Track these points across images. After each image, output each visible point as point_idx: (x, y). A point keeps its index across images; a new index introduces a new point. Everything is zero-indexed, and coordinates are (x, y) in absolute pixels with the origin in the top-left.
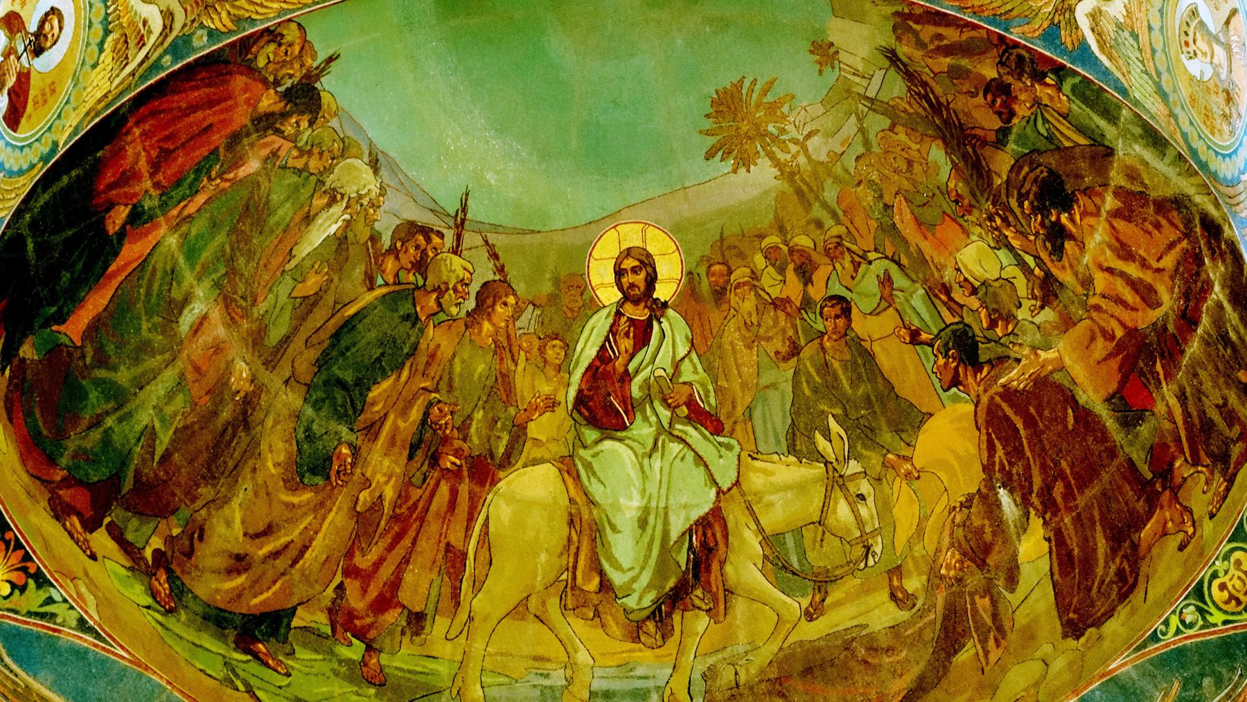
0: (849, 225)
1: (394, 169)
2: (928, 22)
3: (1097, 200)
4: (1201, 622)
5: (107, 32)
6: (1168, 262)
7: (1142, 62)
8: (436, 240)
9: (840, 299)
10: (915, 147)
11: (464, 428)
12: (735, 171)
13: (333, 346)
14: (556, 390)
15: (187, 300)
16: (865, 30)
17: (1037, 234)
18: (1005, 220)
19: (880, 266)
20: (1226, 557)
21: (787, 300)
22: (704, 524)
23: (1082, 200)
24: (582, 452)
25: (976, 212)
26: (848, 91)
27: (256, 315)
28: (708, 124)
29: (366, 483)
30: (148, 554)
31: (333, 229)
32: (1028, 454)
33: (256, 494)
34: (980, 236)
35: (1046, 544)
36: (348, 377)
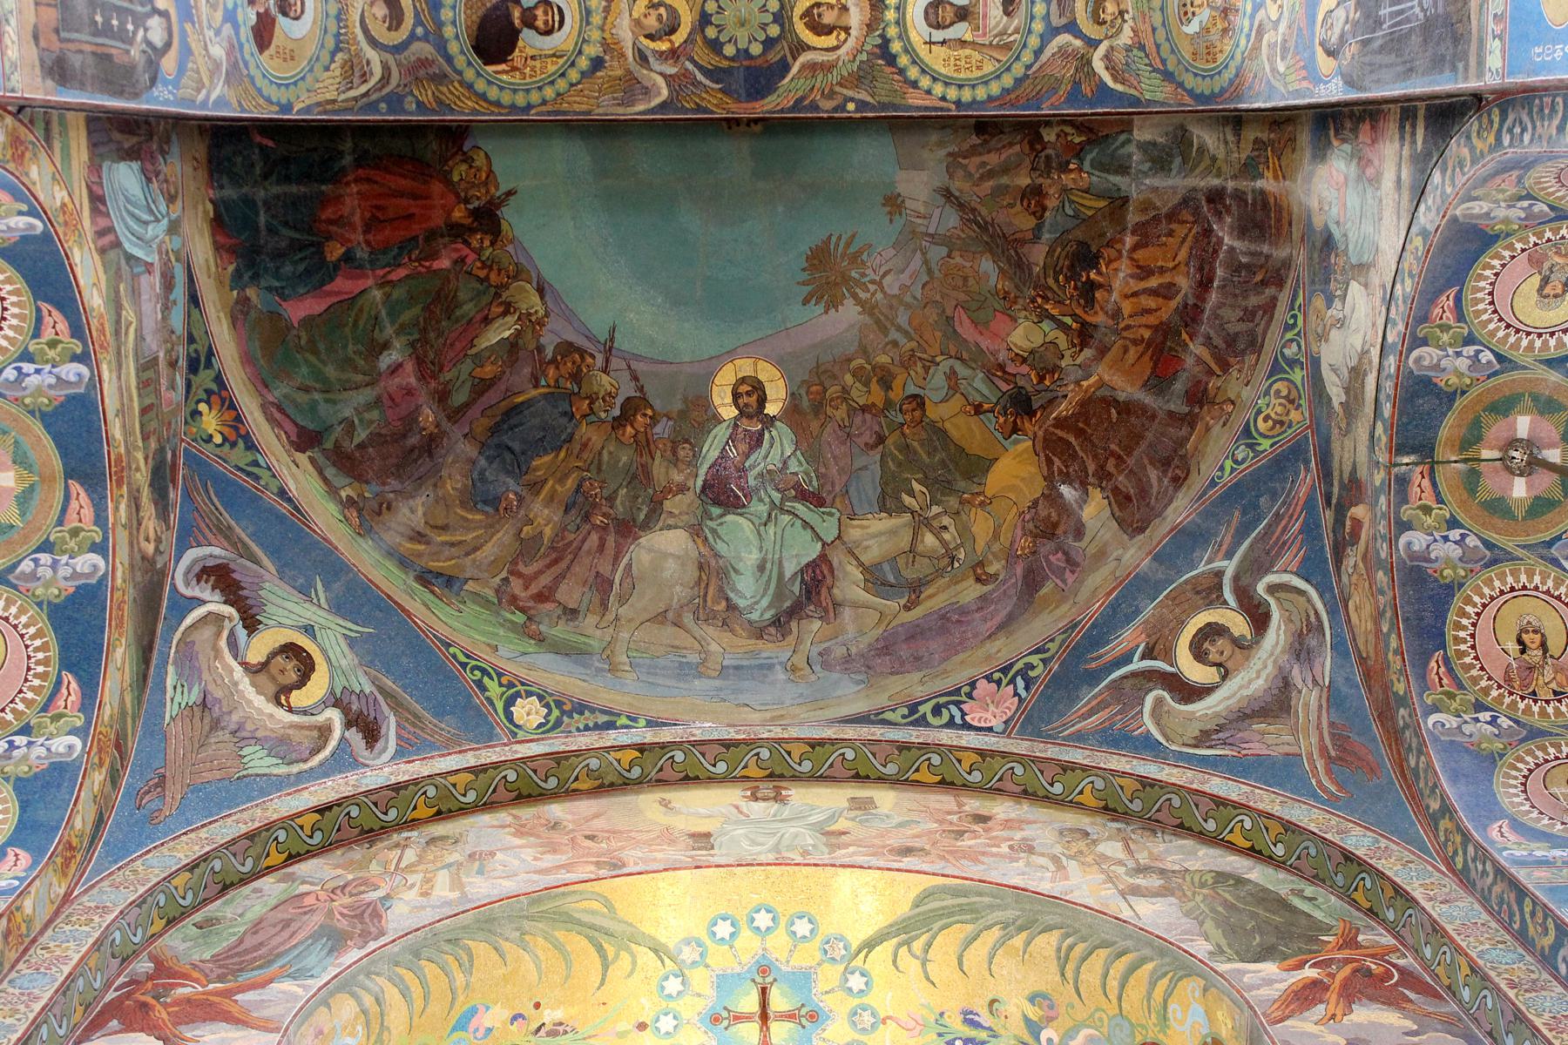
0: (921, 342)
1: (557, 298)
2: (973, 155)
3: (1118, 246)
4: (1251, 455)
5: (337, 49)
6: (1183, 254)
7: (1151, 65)
8: (589, 360)
9: (915, 396)
10: (968, 264)
11: (611, 499)
12: (826, 312)
13: (503, 421)
14: (687, 479)
15: (386, 346)
16: (924, 176)
17: (1071, 298)
18: (1042, 297)
19: (945, 365)
20: (1267, 393)
21: (874, 405)
22: (812, 565)
23: (1106, 252)
24: (709, 523)
25: (1021, 301)
26: (913, 232)
27: (442, 380)
28: (805, 276)
29: (530, 522)
30: (343, 494)
31: (507, 334)
32: (1081, 454)
33: (437, 501)
34: (1026, 317)
35: (1106, 501)
36: (516, 446)
